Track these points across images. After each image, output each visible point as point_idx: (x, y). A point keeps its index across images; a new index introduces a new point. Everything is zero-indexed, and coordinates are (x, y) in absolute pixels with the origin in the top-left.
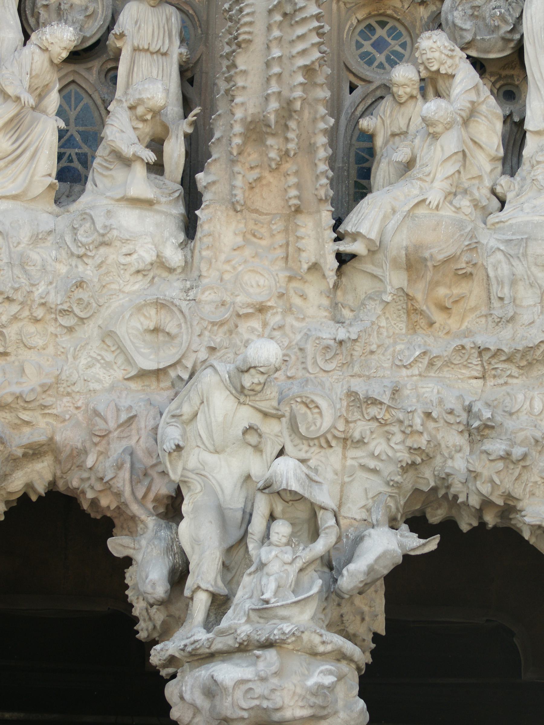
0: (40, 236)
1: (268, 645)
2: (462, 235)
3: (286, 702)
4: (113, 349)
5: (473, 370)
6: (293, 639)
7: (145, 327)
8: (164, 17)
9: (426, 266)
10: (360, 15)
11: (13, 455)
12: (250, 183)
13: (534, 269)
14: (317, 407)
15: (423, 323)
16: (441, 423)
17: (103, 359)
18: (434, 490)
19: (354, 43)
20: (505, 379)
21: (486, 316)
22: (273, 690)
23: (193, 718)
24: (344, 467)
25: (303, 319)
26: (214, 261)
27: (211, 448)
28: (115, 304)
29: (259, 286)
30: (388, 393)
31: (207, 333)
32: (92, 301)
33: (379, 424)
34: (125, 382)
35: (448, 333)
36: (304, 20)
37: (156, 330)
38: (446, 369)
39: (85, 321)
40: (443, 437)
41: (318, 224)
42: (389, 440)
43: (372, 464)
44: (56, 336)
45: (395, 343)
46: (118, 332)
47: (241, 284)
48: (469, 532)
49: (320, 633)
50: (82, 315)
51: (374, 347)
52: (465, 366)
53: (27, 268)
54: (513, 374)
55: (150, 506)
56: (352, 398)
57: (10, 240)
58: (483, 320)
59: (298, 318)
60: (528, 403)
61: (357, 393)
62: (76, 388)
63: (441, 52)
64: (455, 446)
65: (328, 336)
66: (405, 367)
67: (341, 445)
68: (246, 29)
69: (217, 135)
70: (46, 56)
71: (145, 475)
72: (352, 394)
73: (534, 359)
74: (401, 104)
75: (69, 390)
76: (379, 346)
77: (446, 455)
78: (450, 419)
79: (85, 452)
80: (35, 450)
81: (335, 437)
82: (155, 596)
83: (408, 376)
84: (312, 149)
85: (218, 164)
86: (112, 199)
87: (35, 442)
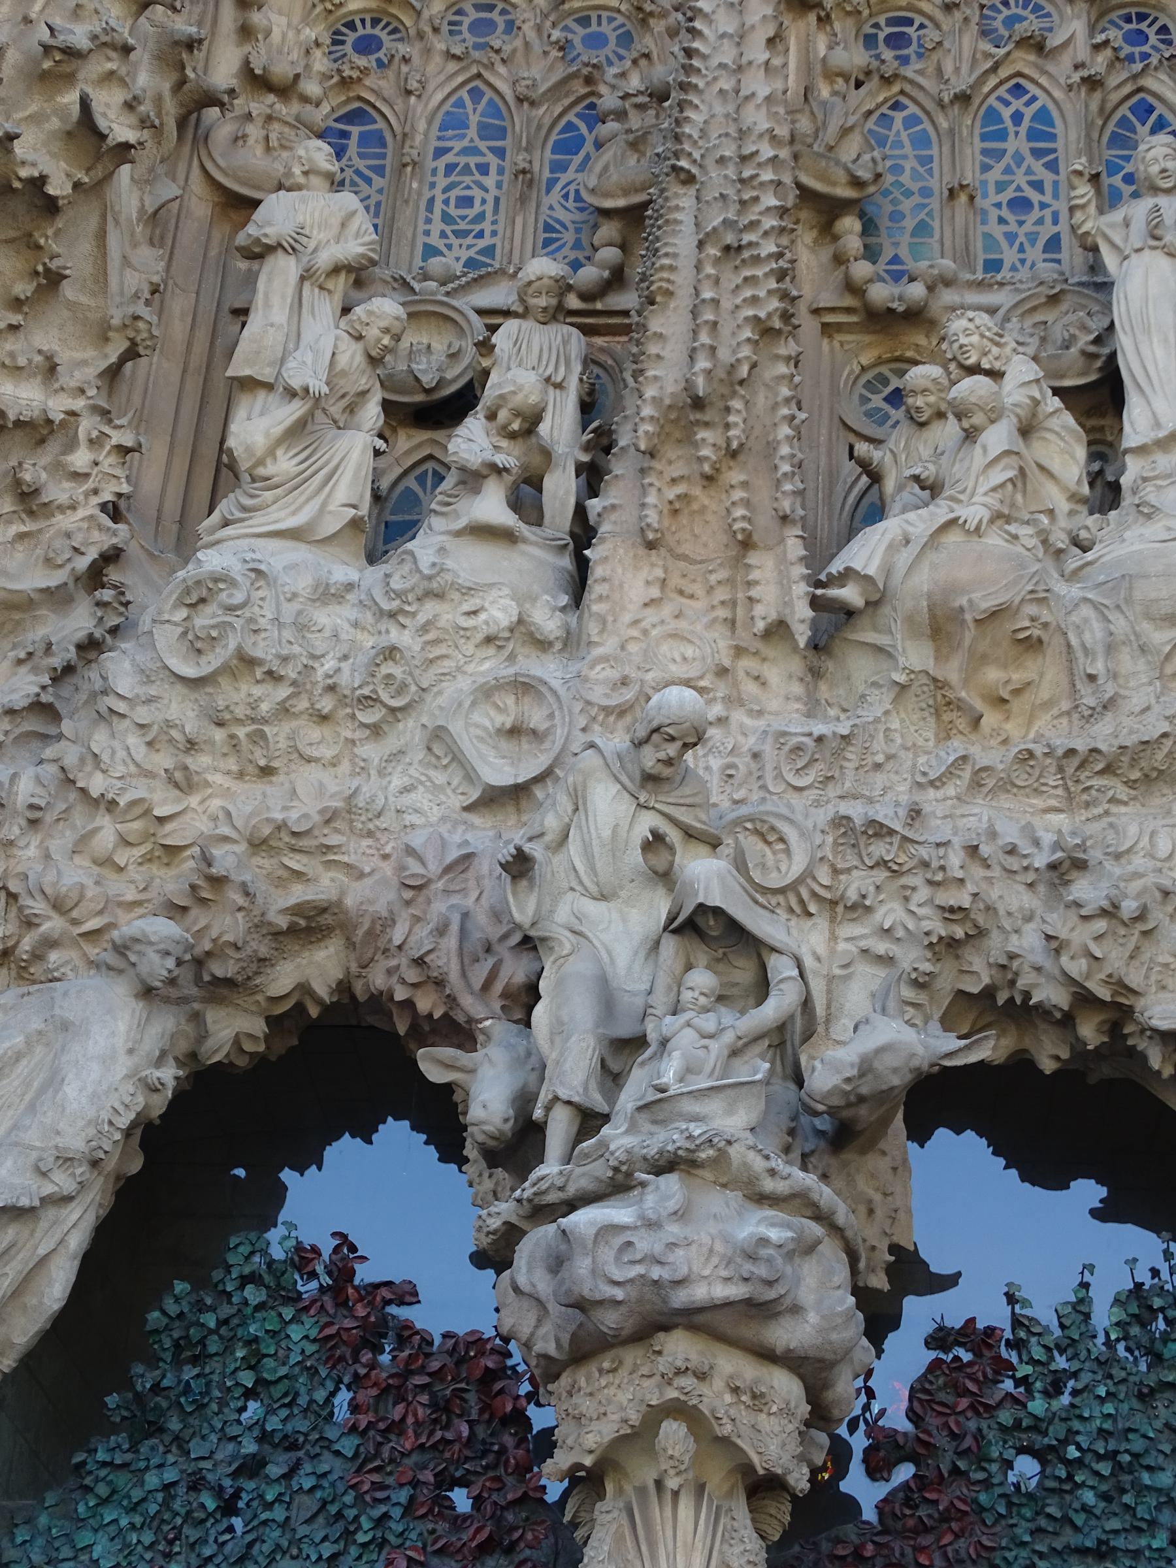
0: (333, 591)
1: (665, 1165)
2: (1022, 577)
3: (695, 1269)
4: (445, 762)
5: (1050, 797)
6: (711, 1152)
7: (498, 725)
8: (559, 337)
9: (963, 622)
10: (866, 359)
11: (270, 924)
12: (671, 502)
13: (1146, 626)
14: (782, 840)
15: (962, 723)
16: (996, 872)
17: (430, 779)
18: (989, 993)
19: (856, 397)
20: (1106, 806)
21: (1068, 713)
22: (672, 1246)
23: (536, 1327)
24: (833, 952)
25: (760, 713)
26: (610, 619)
27: (593, 889)
28: (449, 689)
29: (685, 659)
30: (902, 813)
31: (596, 727)
32: (409, 680)
33: (888, 874)
34: (465, 814)
35: (1005, 742)
36: (756, 260)
37: (514, 732)
38: (1003, 796)
39: (399, 715)
40: (1001, 897)
41: (782, 560)
42: (907, 899)
43: (881, 947)
44: (353, 742)
45: (916, 755)
46: (450, 727)
47: (655, 655)
48: (1055, 1073)
49: (766, 1152)
50: (394, 703)
51: (880, 758)
52: (1036, 790)
53: (309, 635)
54: (1118, 796)
55: (497, 1005)
56: (843, 830)
57: (280, 589)
58: (1064, 721)
59: (752, 710)
60: (1147, 839)
61: (848, 818)
62: (382, 823)
63: (982, 336)
64: (1021, 909)
65: (799, 730)
66: (932, 783)
67: (827, 914)
68: (665, 275)
69: (622, 443)
70: (358, 347)
71: (488, 950)
72: (840, 822)
73: (1155, 769)
74: (922, 425)
75: (371, 826)
76: (890, 757)
77: (1009, 928)
78: (1014, 863)
79: (389, 922)
80: (308, 918)
81: (814, 894)
82: (486, 1128)
83: (937, 801)
84: (771, 447)
85: (621, 484)
86: (448, 533)
87: (308, 902)
